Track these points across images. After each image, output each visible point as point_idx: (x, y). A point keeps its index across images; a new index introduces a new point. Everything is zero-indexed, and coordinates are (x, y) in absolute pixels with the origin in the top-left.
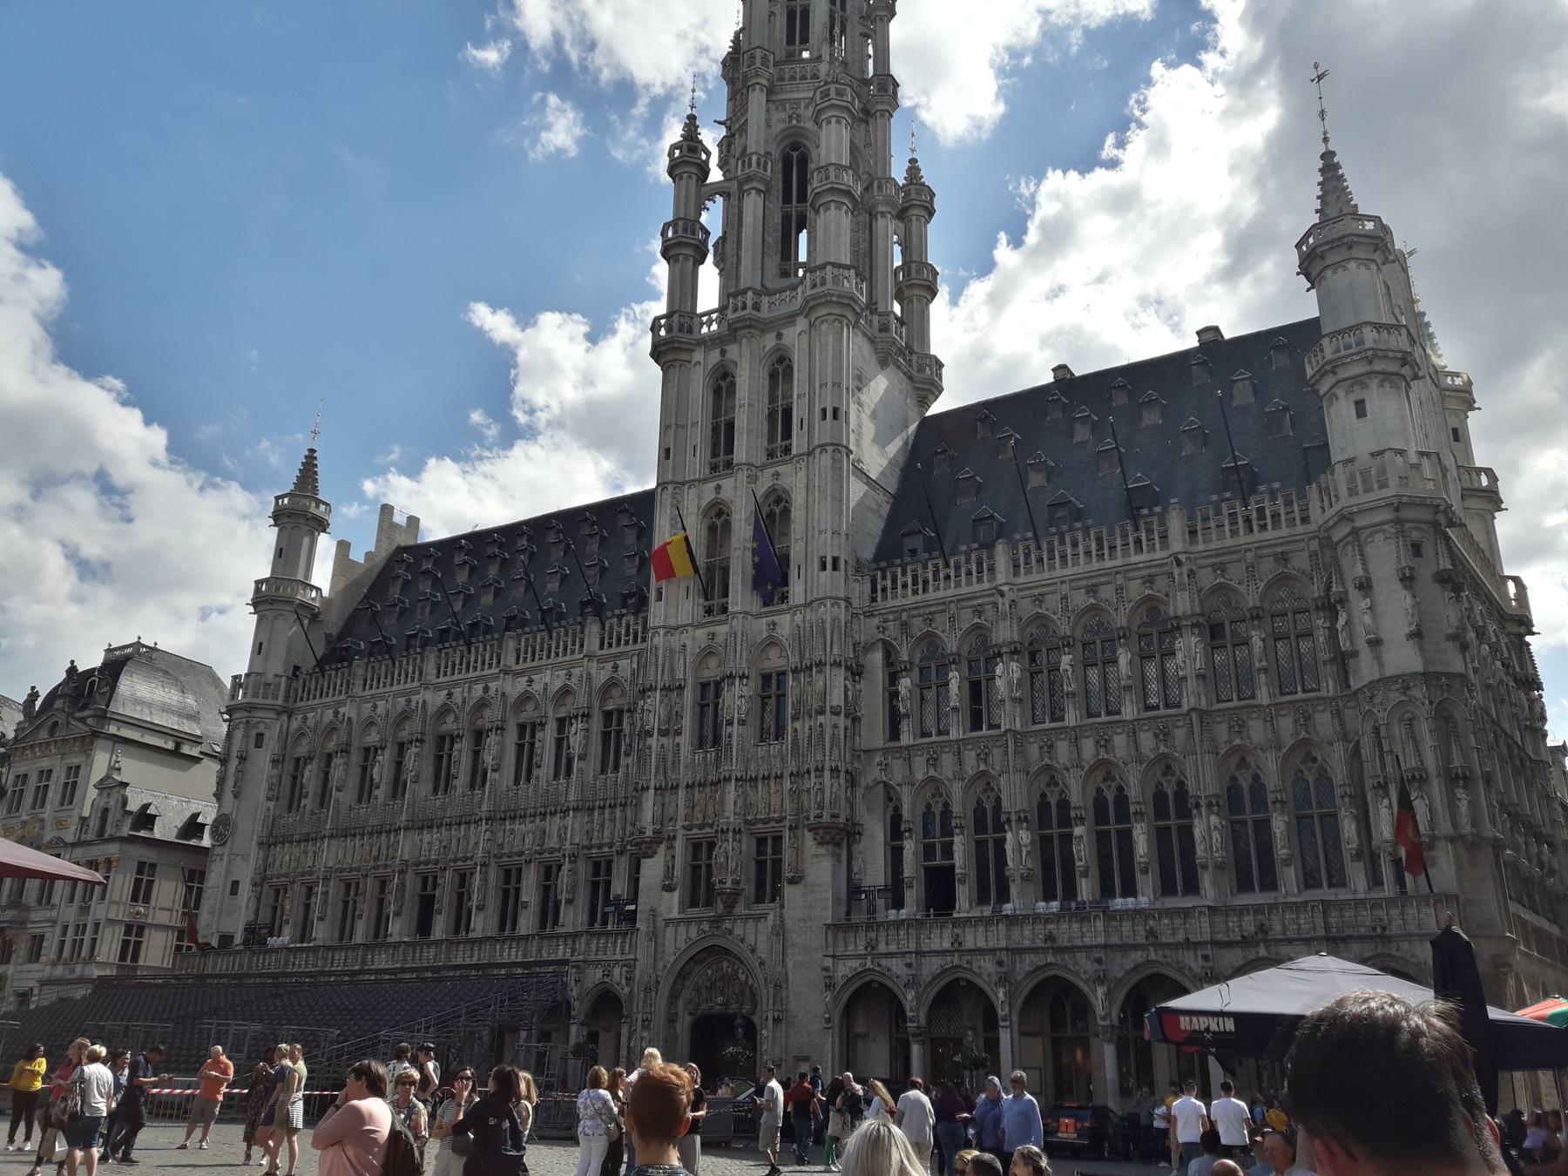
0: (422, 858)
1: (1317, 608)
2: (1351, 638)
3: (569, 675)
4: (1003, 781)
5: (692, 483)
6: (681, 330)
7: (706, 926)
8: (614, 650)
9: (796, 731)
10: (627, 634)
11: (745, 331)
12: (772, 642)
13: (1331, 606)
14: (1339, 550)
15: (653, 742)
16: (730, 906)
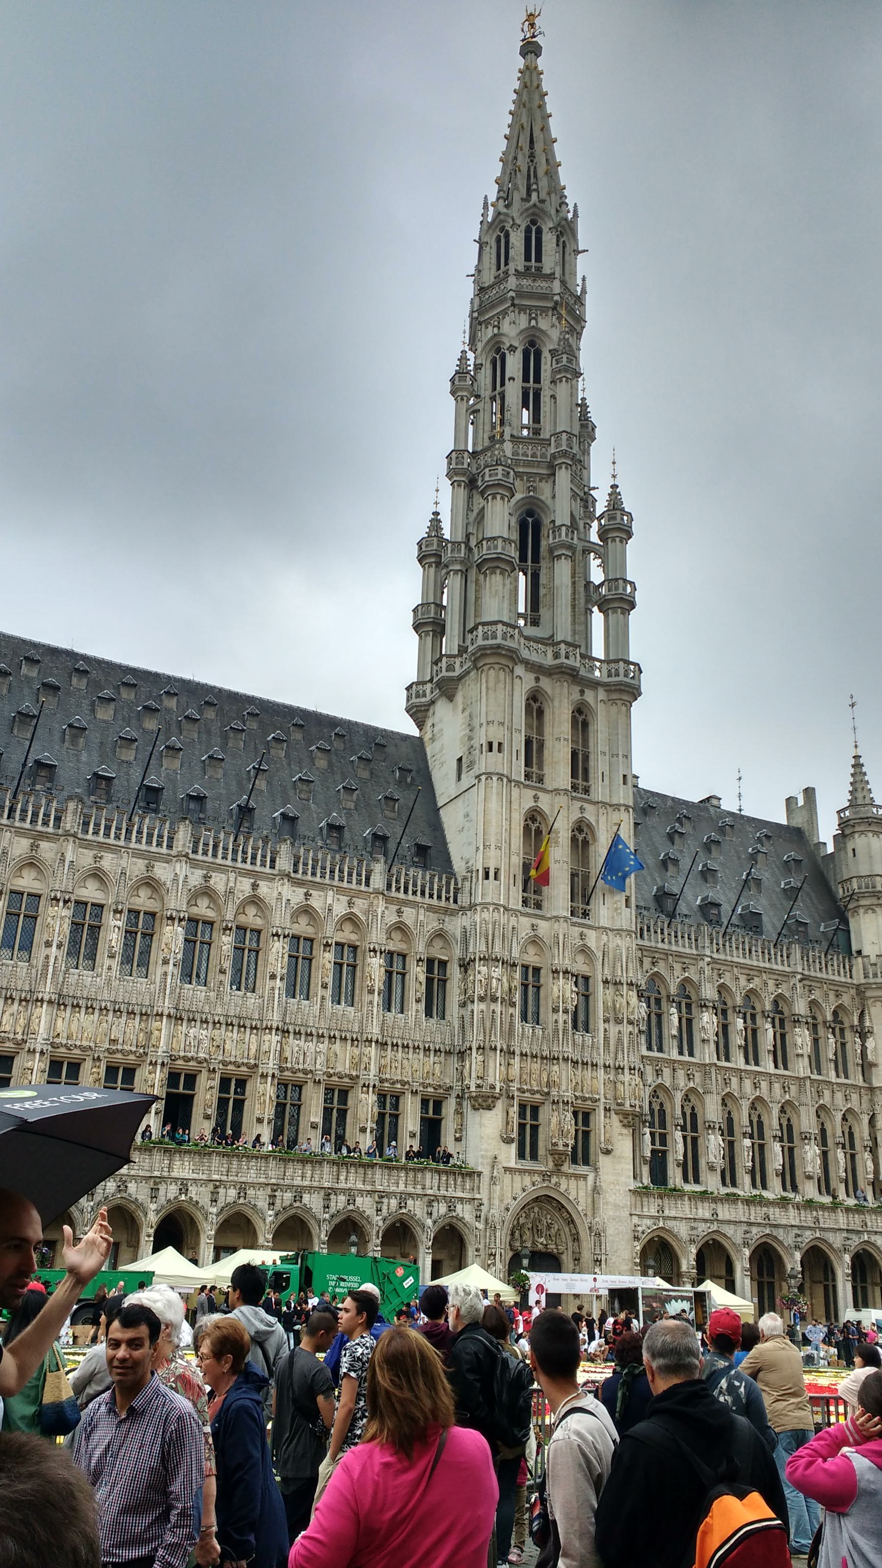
0: (182, 1054)
1: (857, 1031)
2: (876, 1056)
3: (350, 904)
4: (708, 1098)
5: (518, 783)
6: (504, 638)
7: (536, 1178)
8: (401, 895)
9: (605, 1031)
10: (415, 885)
11: (567, 677)
12: (585, 950)
13: (863, 1034)
14: (870, 1002)
15: (498, 1007)
16: (558, 1165)
